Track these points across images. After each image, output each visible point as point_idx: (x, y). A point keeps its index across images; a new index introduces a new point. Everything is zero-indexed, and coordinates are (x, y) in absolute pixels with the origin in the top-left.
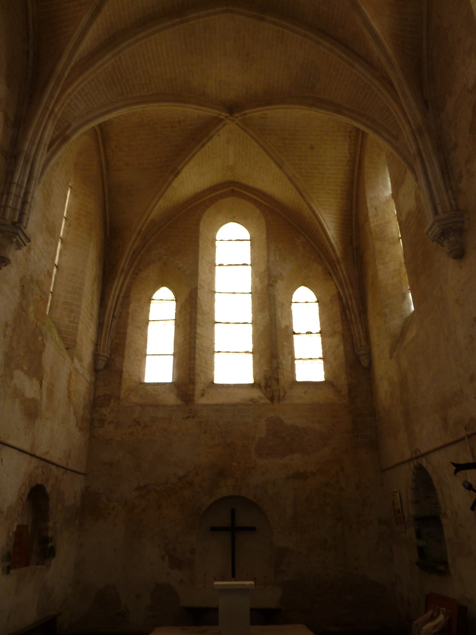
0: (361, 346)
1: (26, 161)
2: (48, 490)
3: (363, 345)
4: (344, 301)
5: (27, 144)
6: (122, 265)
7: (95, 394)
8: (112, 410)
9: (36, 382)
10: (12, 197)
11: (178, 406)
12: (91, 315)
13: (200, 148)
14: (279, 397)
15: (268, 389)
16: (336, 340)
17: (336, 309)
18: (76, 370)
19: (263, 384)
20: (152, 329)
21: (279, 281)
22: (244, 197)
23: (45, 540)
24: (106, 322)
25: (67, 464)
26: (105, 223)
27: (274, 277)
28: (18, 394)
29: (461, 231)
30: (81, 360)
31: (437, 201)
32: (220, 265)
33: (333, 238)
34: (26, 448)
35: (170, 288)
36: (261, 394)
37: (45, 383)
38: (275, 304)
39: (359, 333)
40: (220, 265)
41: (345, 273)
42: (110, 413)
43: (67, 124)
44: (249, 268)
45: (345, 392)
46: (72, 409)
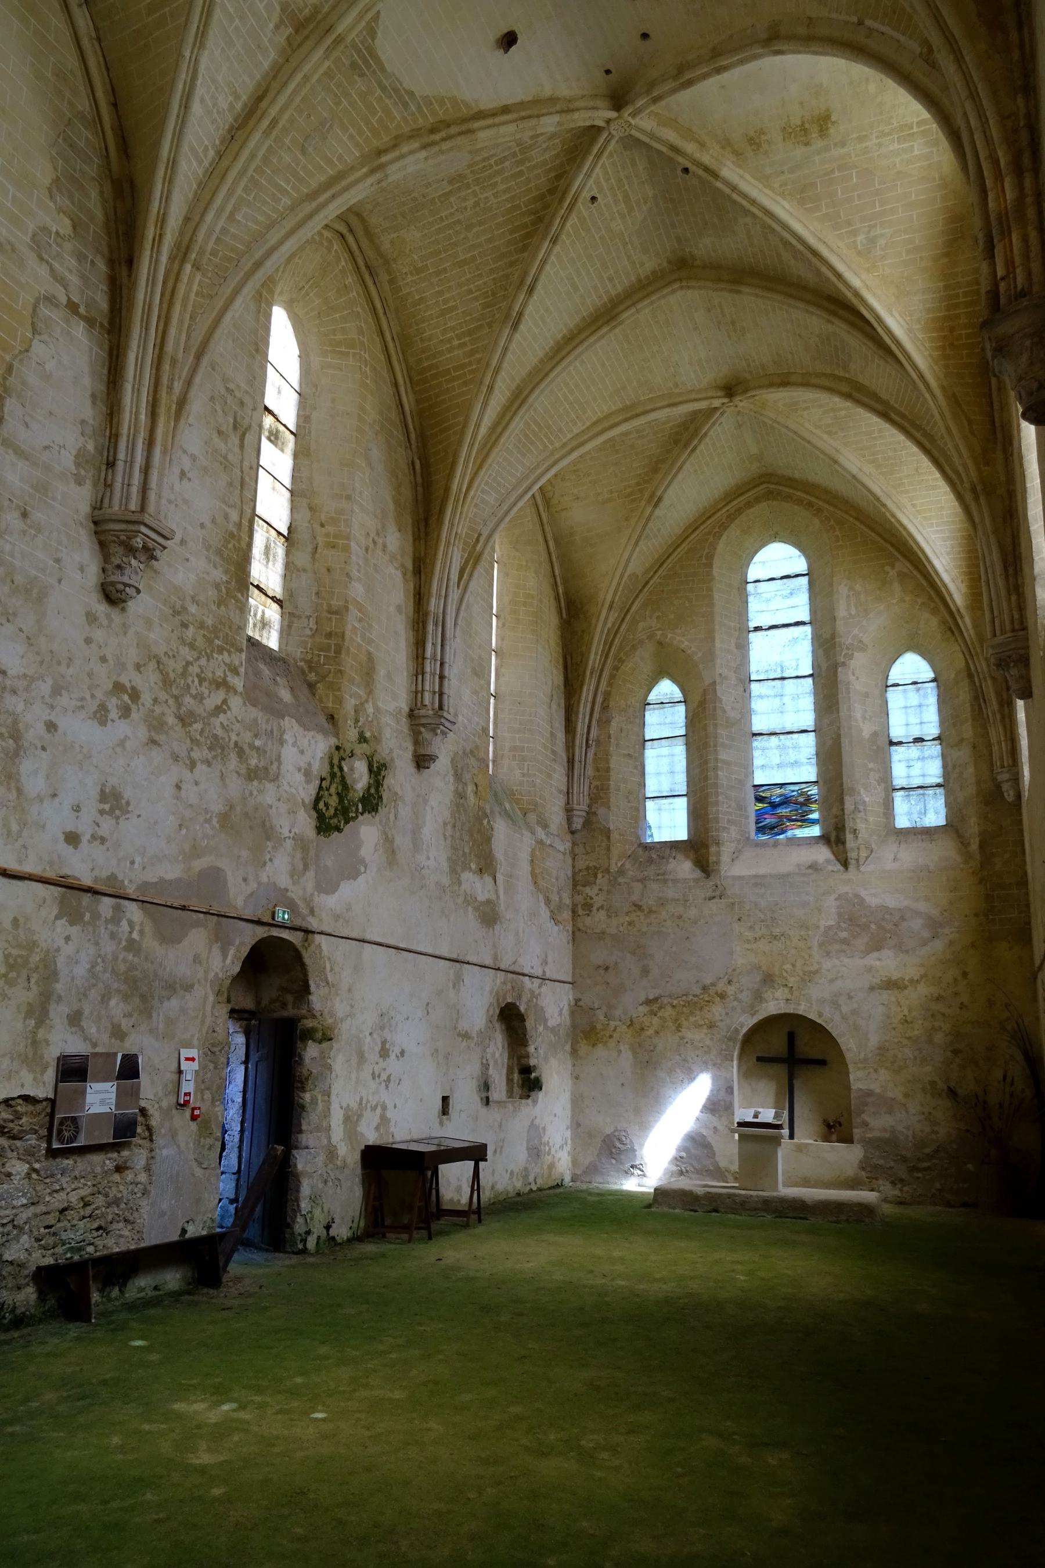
0: (1003, 766)
1: (436, 624)
2: (522, 1009)
3: (1006, 764)
4: (977, 684)
5: (433, 601)
6: (590, 663)
7: (574, 867)
8: (600, 890)
9: (488, 879)
10: (428, 676)
11: (696, 880)
12: (554, 752)
13: (689, 455)
14: (857, 860)
15: (841, 847)
16: (963, 754)
17: (964, 696)
18: (541, 842)
19: (833, 838)
20: (651, 754)
21: (856, 654)
22: (788, 498)
23: (526, 1070)
24: (577, 758)
25: (544, 972)
26: (557, 598)
27: (847, 648)
28: (469, 900)
29: (1024, 661)
30: (545, 826)
31: (996, 613)
32: (757, 629)
33: (946, 571)
34: (488, 962)
35: (675, 681)
36: (830, 856)
37: (500, 877)
38: (849, 698)
39: (1000, 743)
40: (757, 629)
41: (972, 632)
42: (597, 895)
43: (476, 536)
44: (808, 629)
45: (974, 847)
46: (541, 897)
